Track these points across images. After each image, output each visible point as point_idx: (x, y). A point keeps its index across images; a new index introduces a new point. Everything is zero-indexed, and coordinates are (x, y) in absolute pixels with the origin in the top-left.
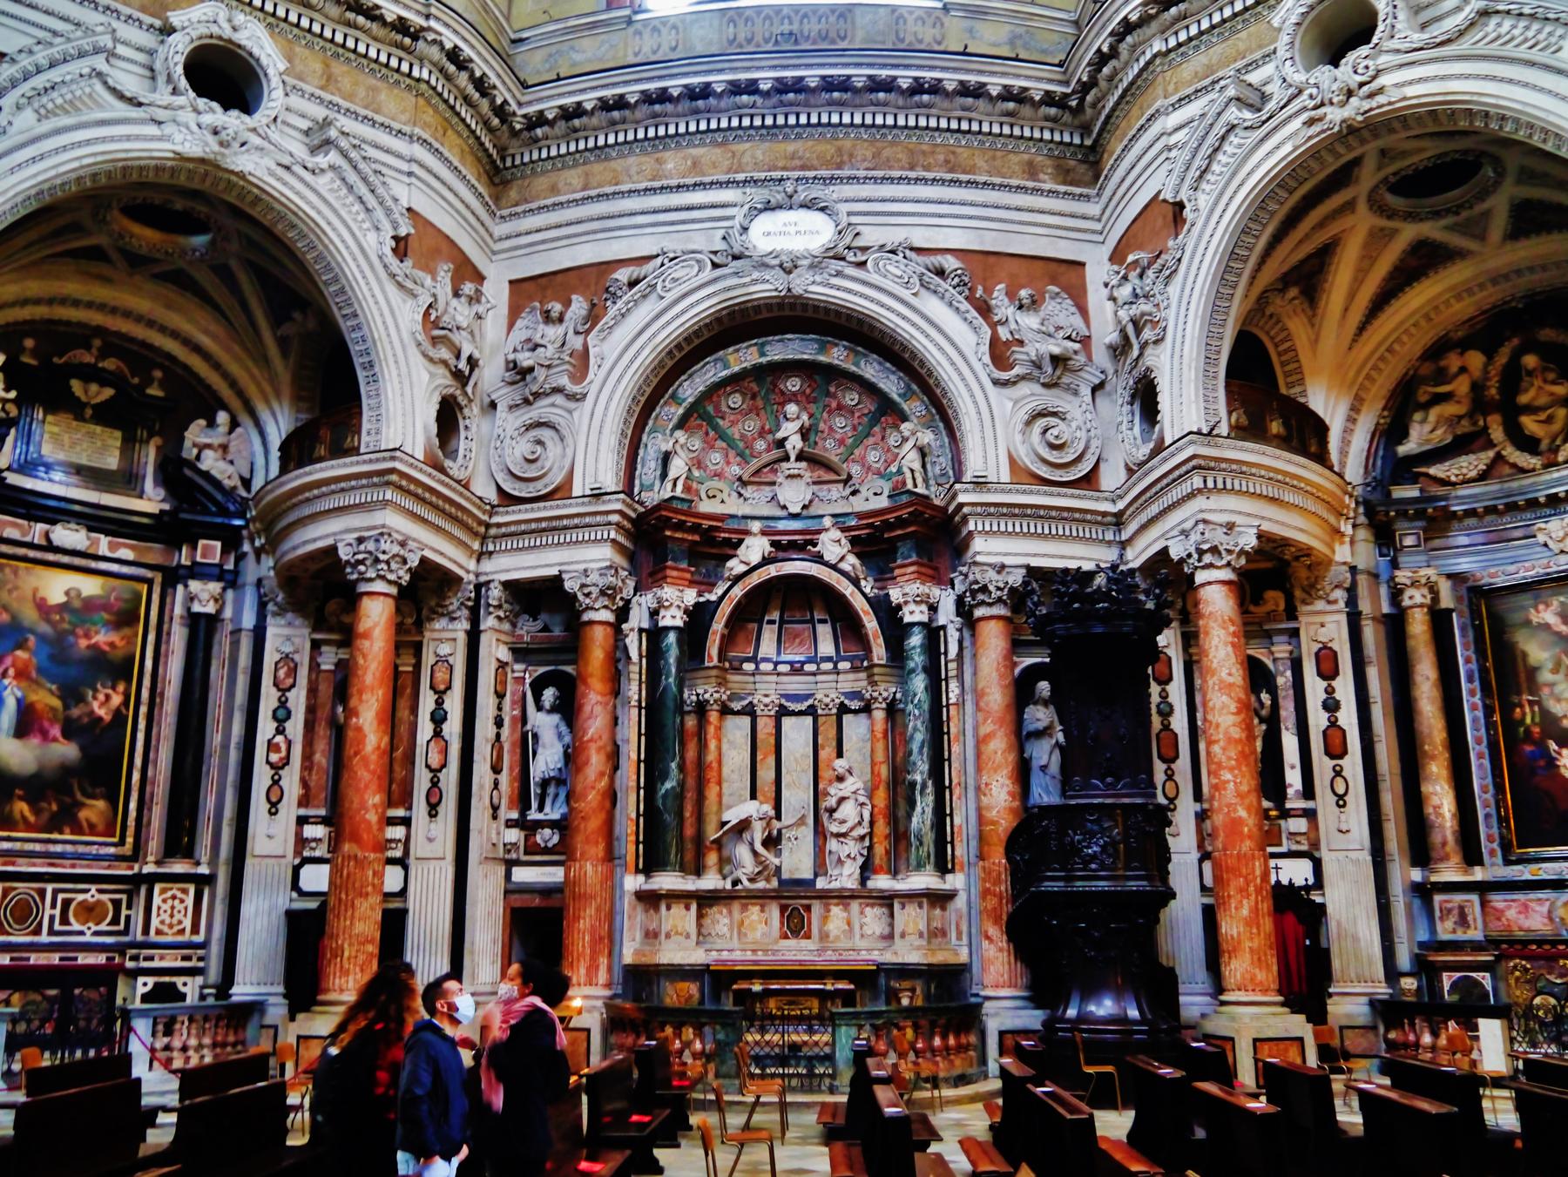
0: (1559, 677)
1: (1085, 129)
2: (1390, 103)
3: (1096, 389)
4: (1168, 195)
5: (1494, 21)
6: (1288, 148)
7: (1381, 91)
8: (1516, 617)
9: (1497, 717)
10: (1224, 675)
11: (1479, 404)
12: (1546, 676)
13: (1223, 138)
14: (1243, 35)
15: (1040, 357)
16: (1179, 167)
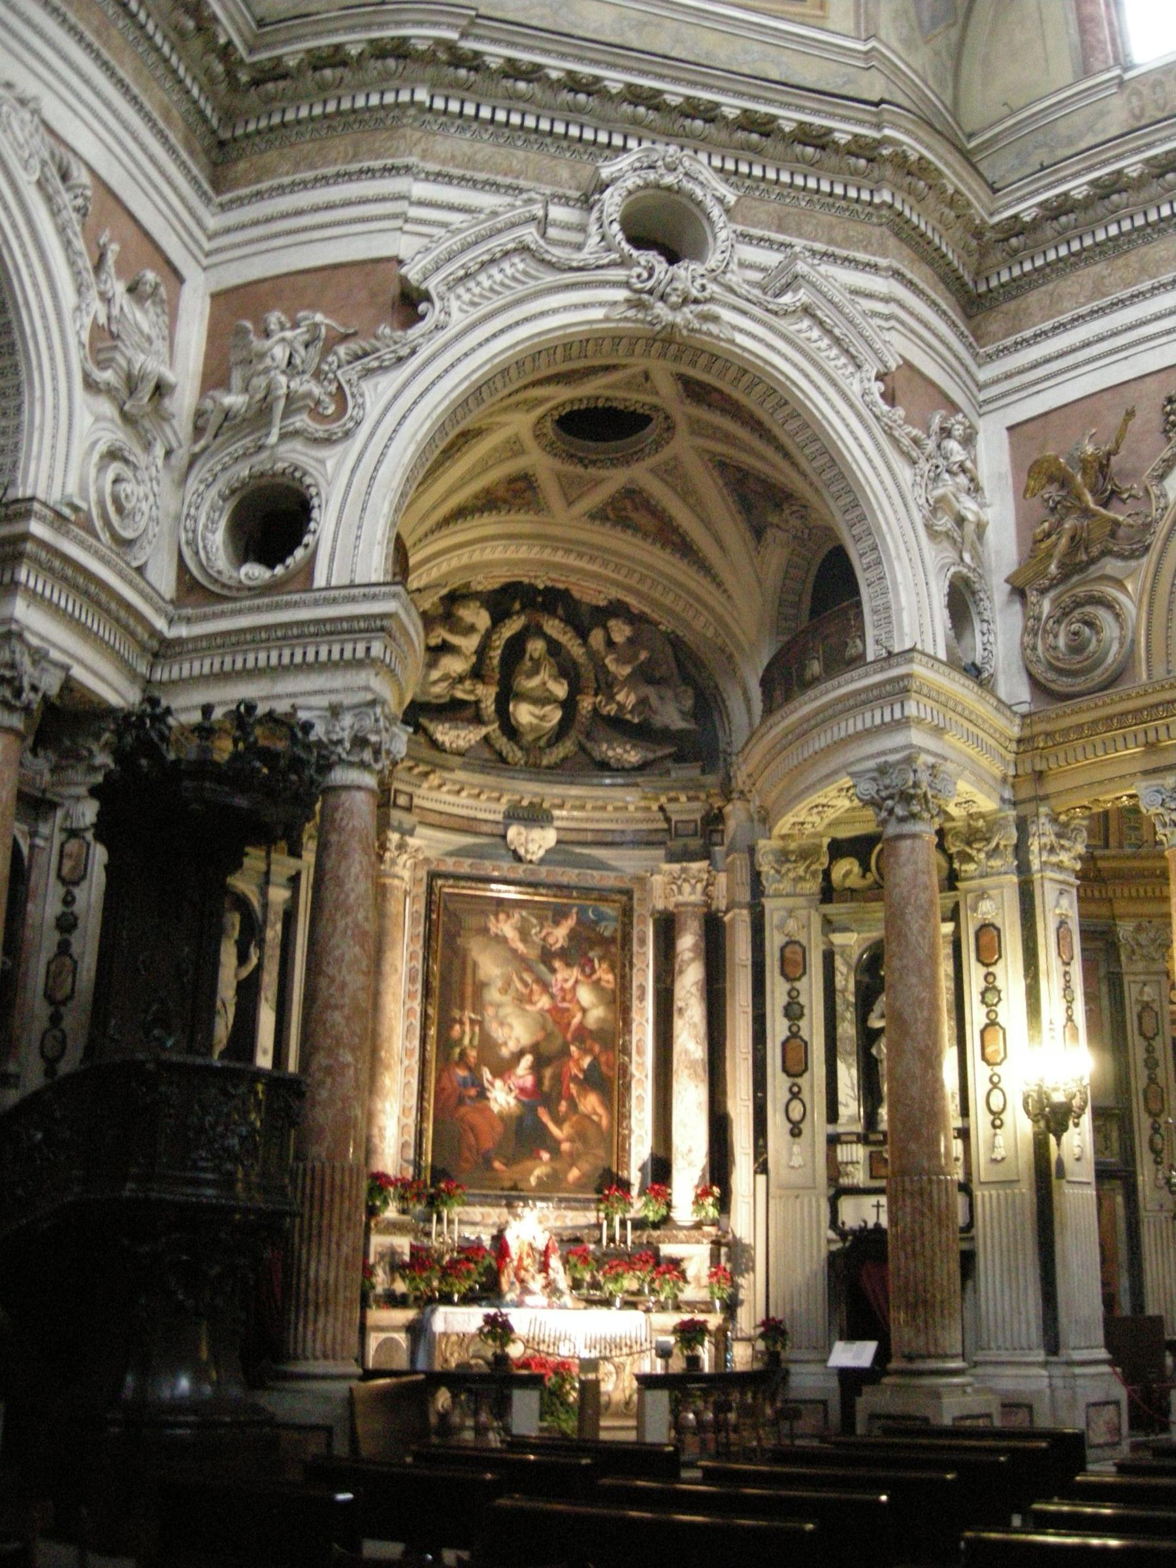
0: (507, 999)
1: (229, 116)
2: (718, 337)
3: (169, 453)
4: (413, 273)
5: (806, 323)
6: (598, 314)
7: (715, 319)
8: (472, 921)
9: (433, 1032)
10: (360, 916)
11: (477, 673)
12: (493, 995)
13: (506, 254)
14: (521, 154)
15: (143, 377)
16: (440, 251)
